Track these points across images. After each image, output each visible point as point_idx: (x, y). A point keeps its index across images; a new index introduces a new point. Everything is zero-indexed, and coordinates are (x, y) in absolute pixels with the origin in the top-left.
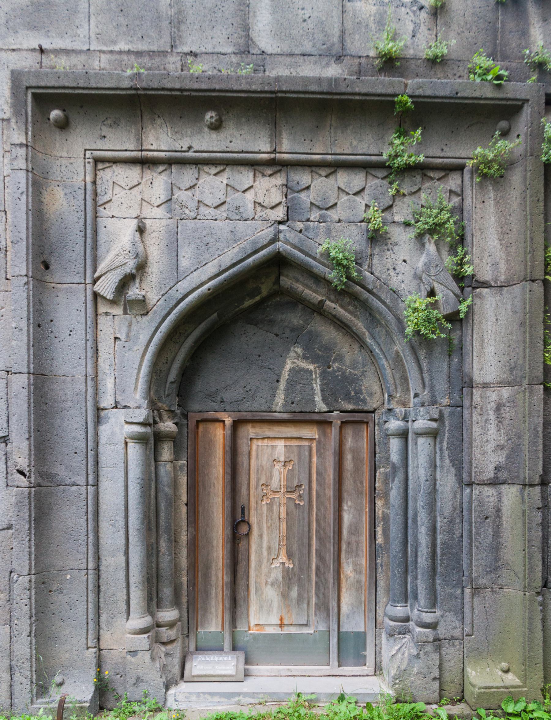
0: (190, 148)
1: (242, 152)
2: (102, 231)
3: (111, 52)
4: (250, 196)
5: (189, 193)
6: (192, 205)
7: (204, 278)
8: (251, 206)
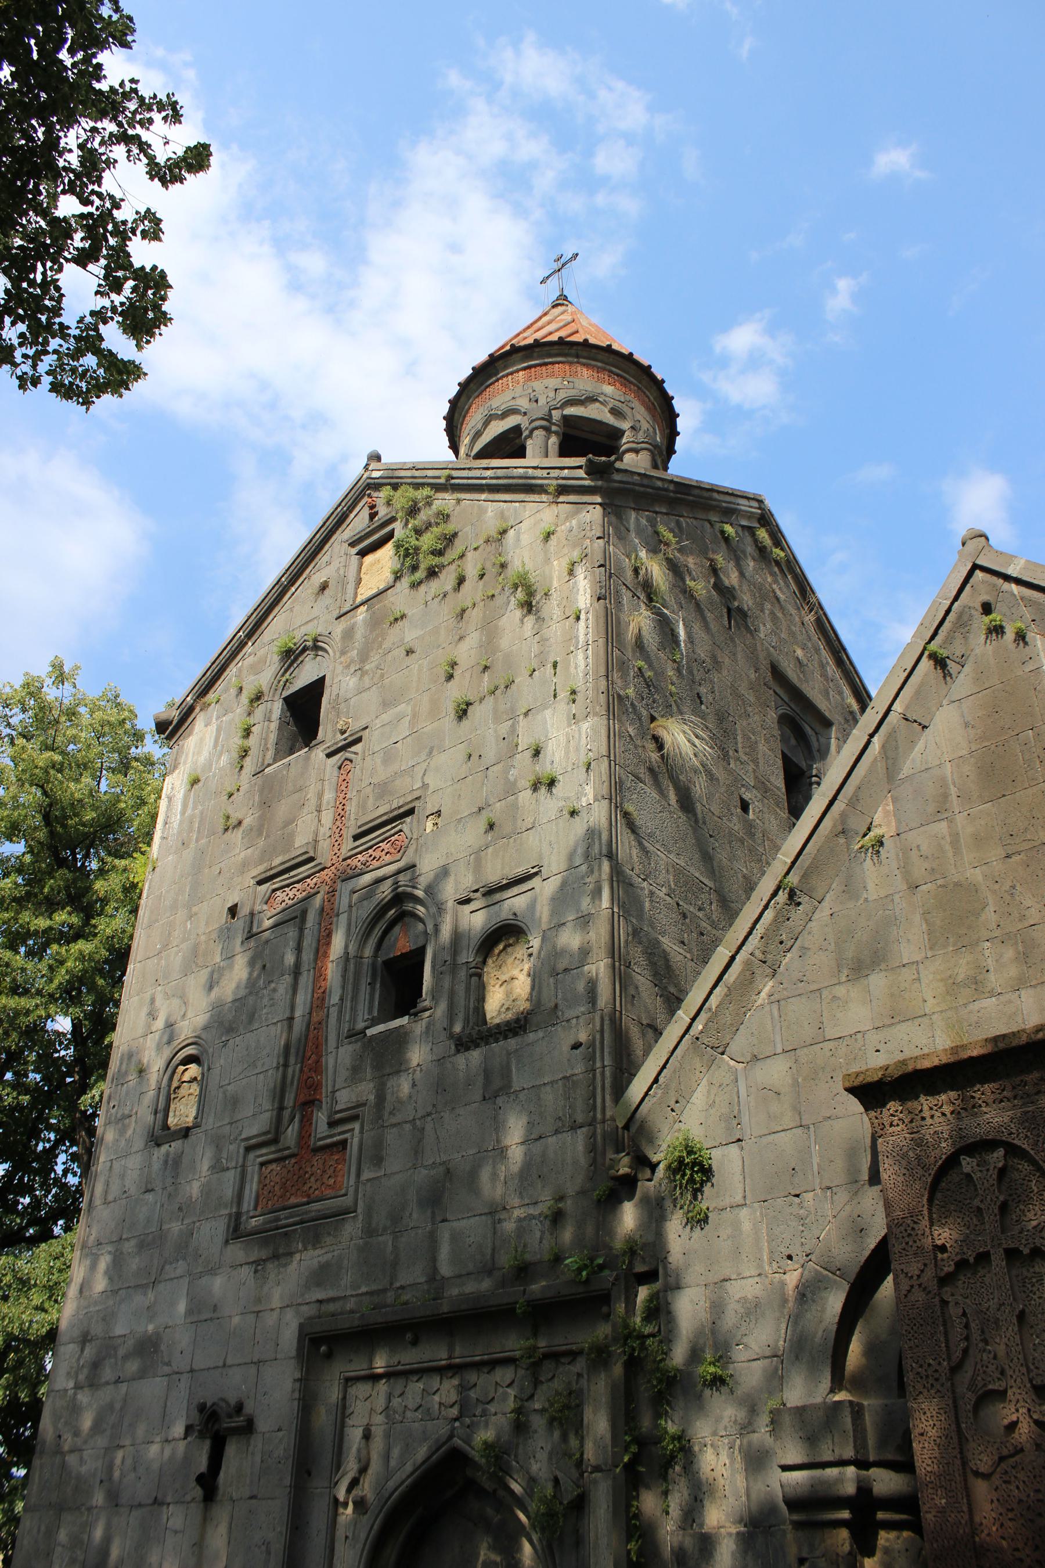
0: (399, 1362)
1: (431, 1361)
2: (346, 1438)
3: (357, 1295)
4: (437, 1398)
5: (399, 1400)
6: (400, 1410)
7: (404, 1477)
8: (437, 1406)
